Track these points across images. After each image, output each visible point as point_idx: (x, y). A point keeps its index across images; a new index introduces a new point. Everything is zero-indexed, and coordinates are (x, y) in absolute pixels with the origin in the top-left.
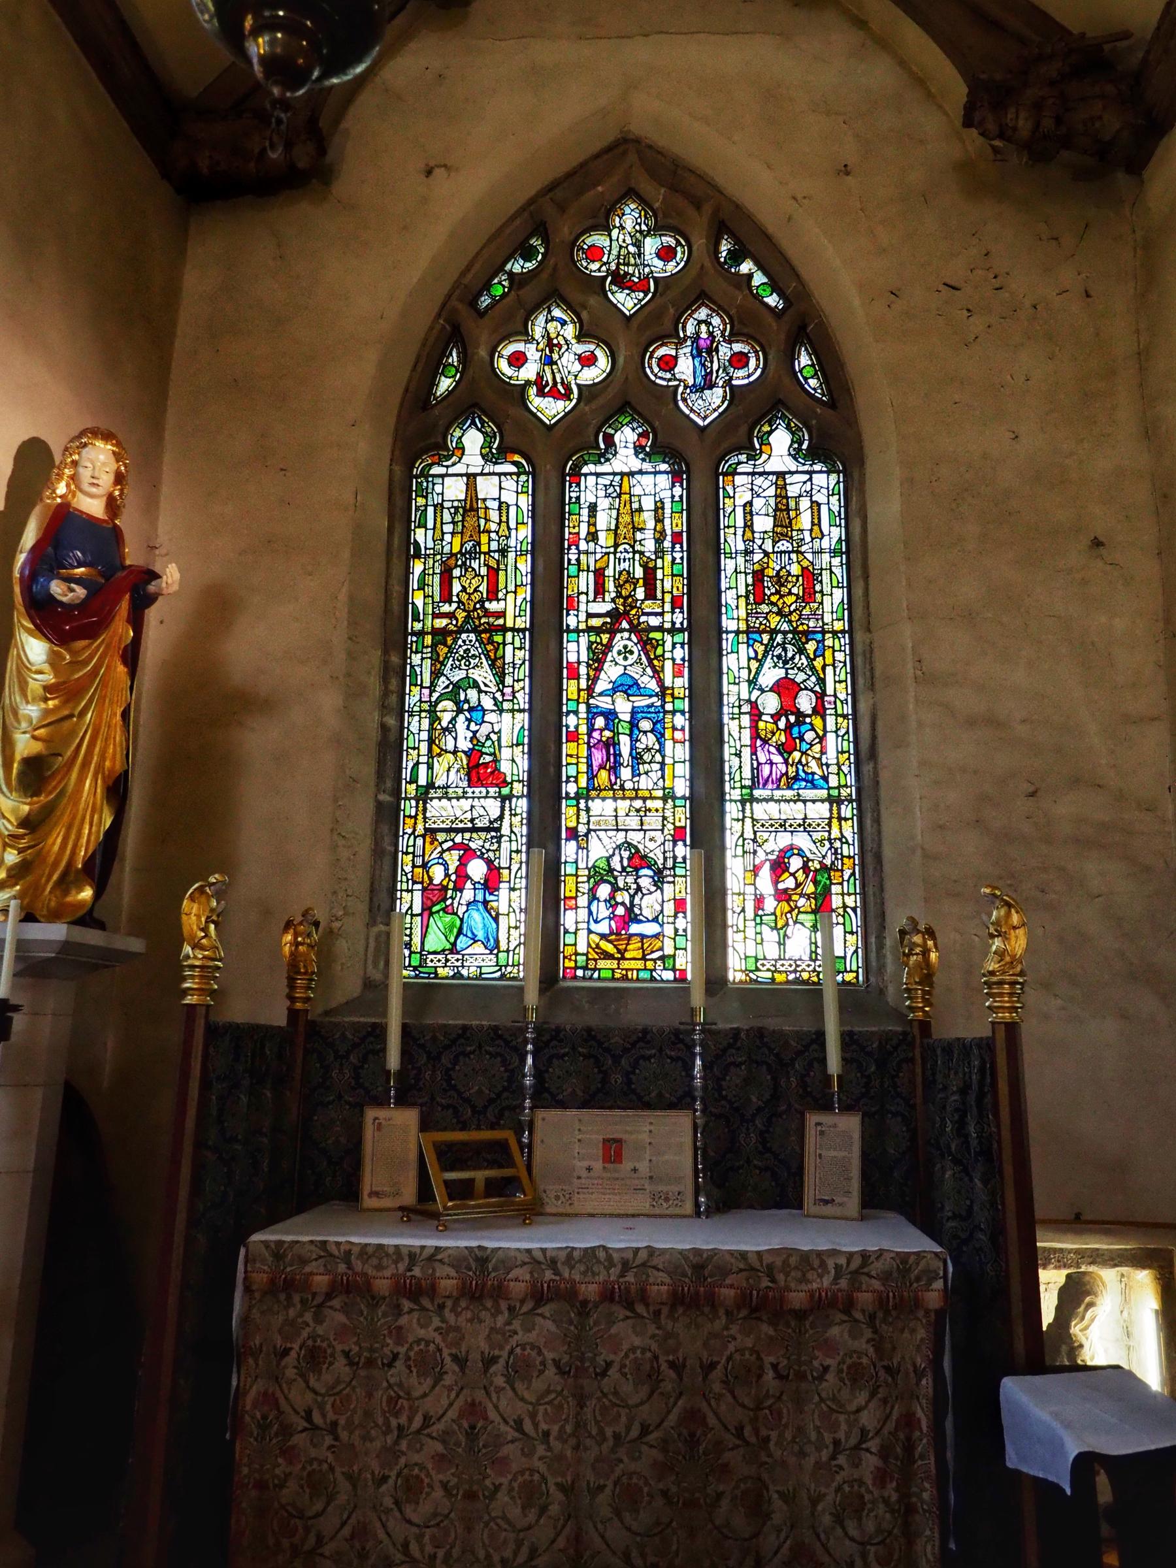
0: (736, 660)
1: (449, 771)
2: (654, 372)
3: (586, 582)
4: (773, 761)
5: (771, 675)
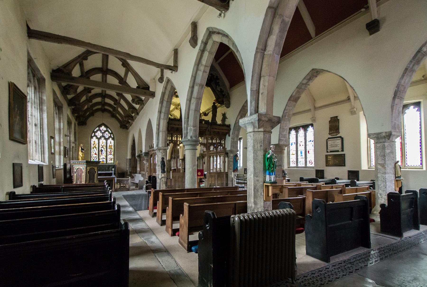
0: (108, 149)
1: (94, 154)
2: (104, 135)
3: (101, 145)
4: (110, 154)
5: (110, 150)
